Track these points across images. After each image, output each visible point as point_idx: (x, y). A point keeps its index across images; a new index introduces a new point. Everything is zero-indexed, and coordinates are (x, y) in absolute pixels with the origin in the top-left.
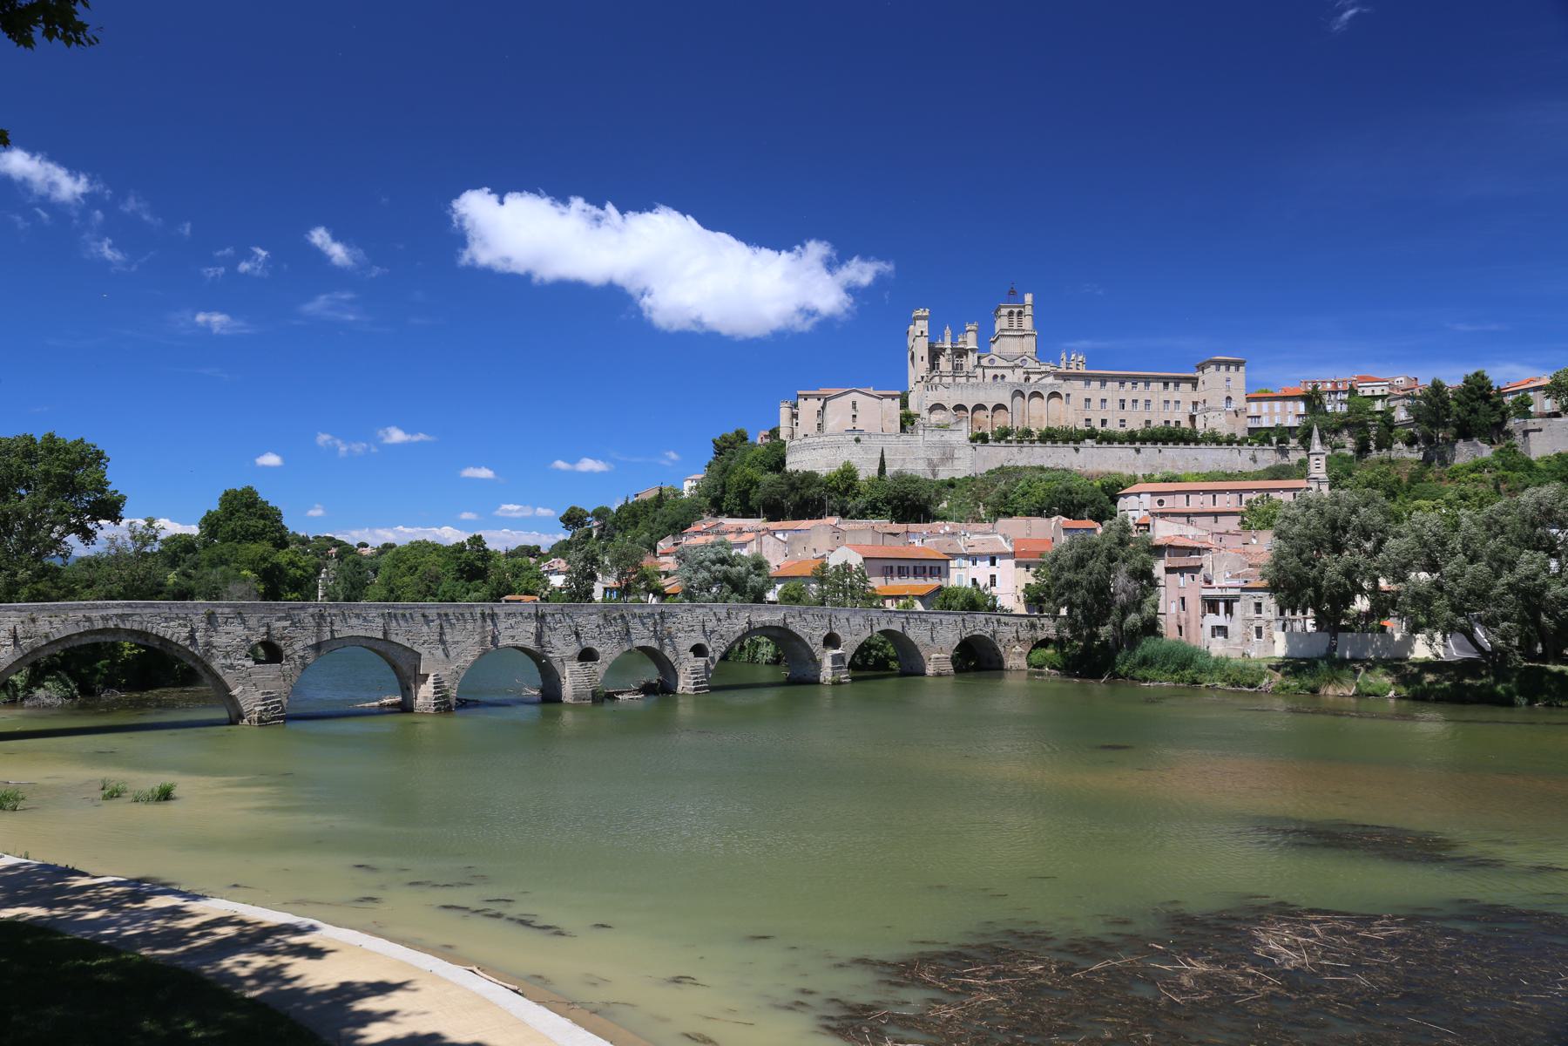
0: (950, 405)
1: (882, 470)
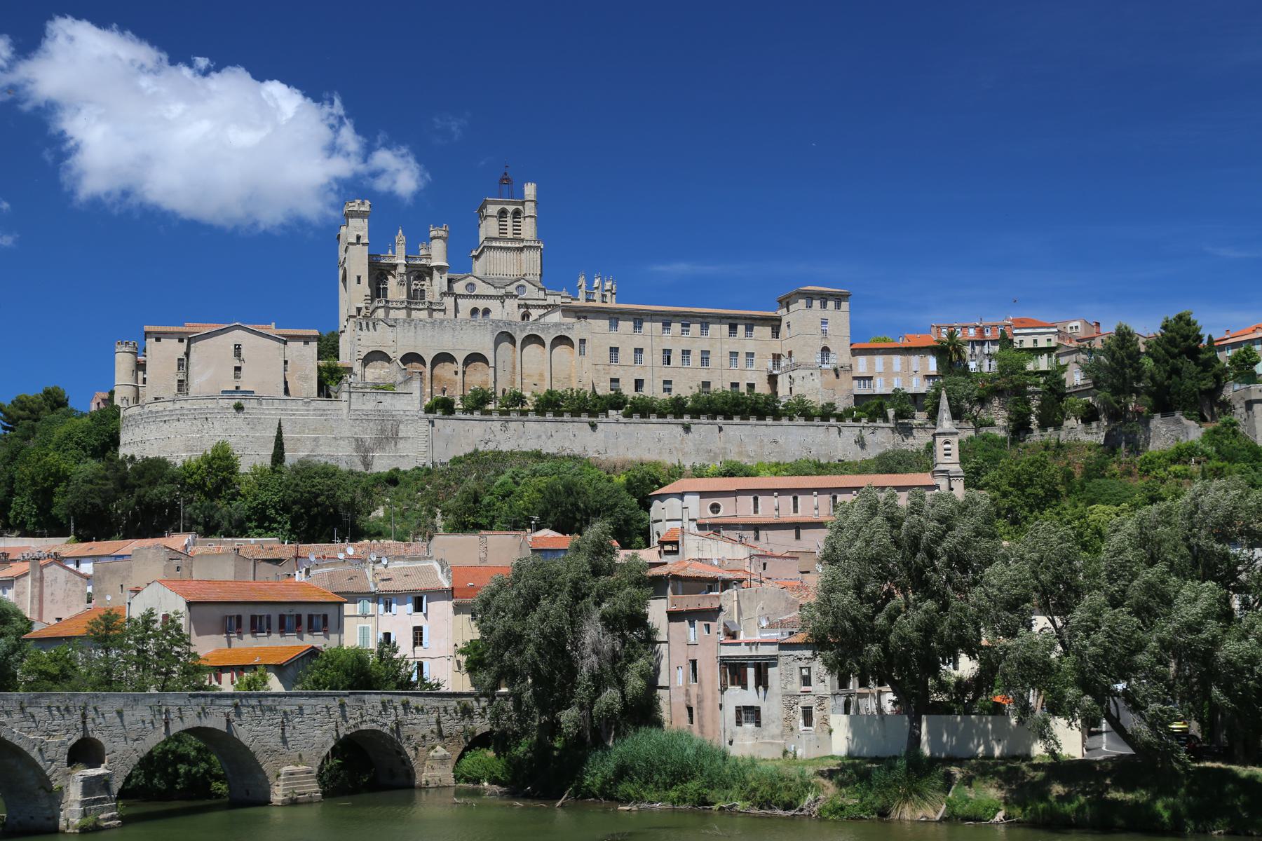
0: (397, 353)
1: (278, 456)
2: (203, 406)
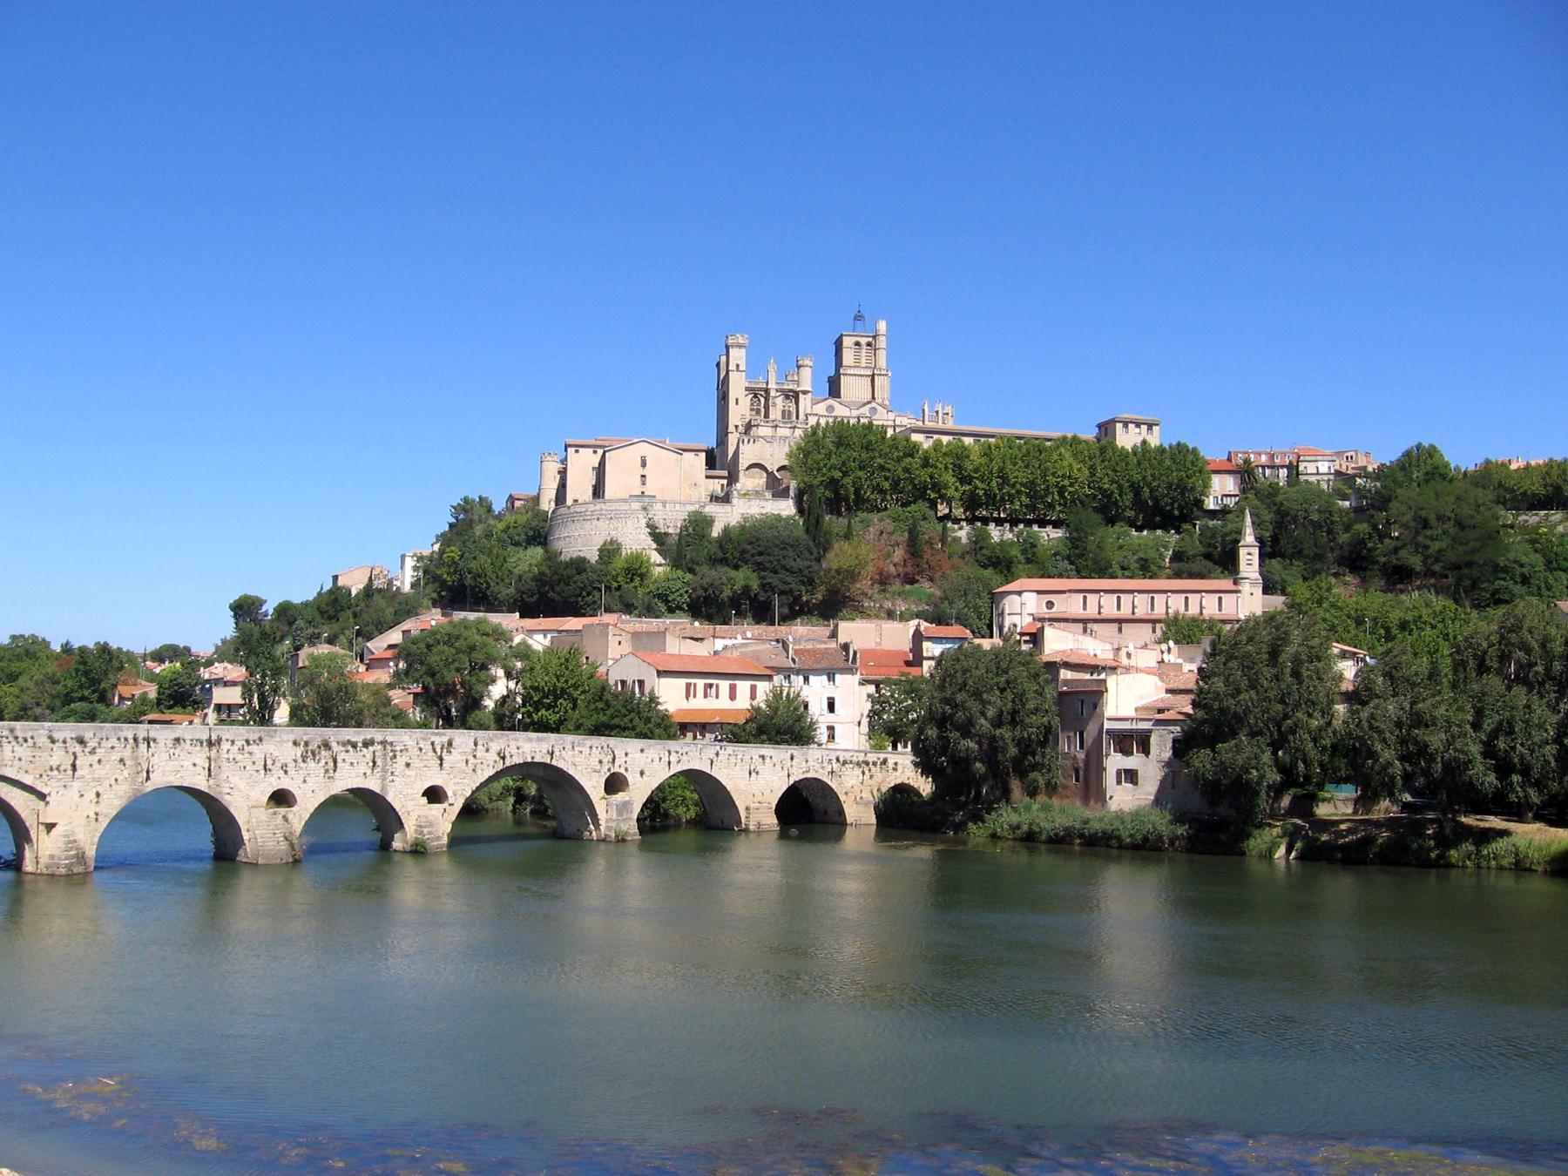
2: (618, 507)
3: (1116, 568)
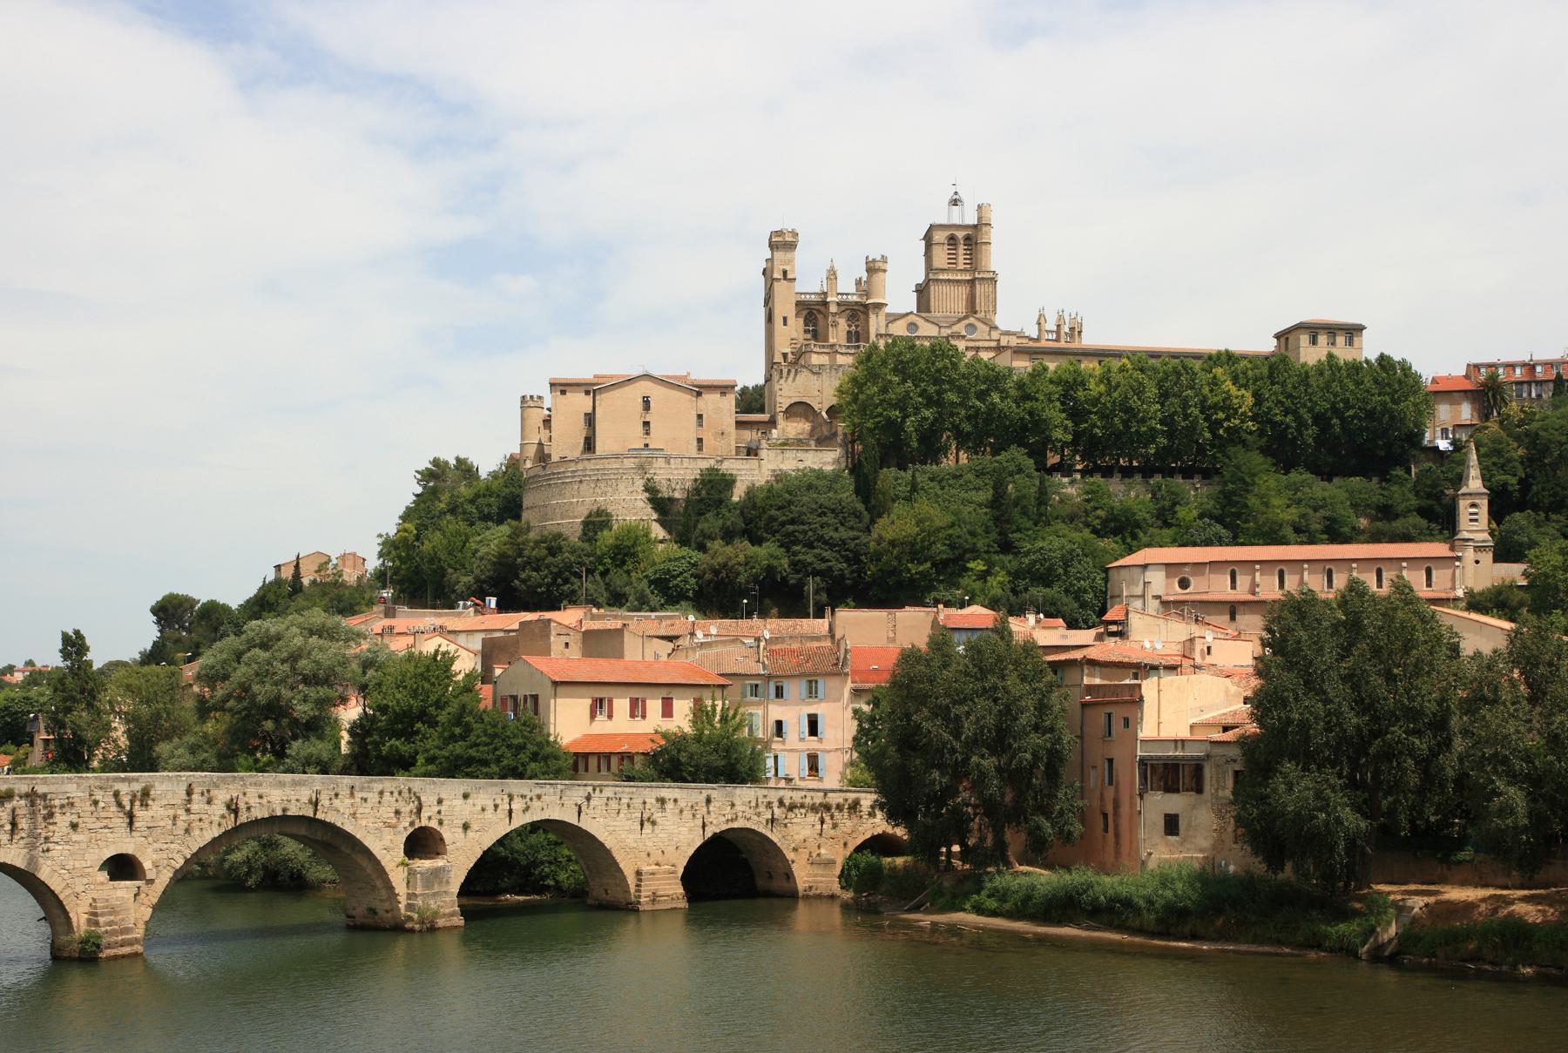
3: (1288, 531)
